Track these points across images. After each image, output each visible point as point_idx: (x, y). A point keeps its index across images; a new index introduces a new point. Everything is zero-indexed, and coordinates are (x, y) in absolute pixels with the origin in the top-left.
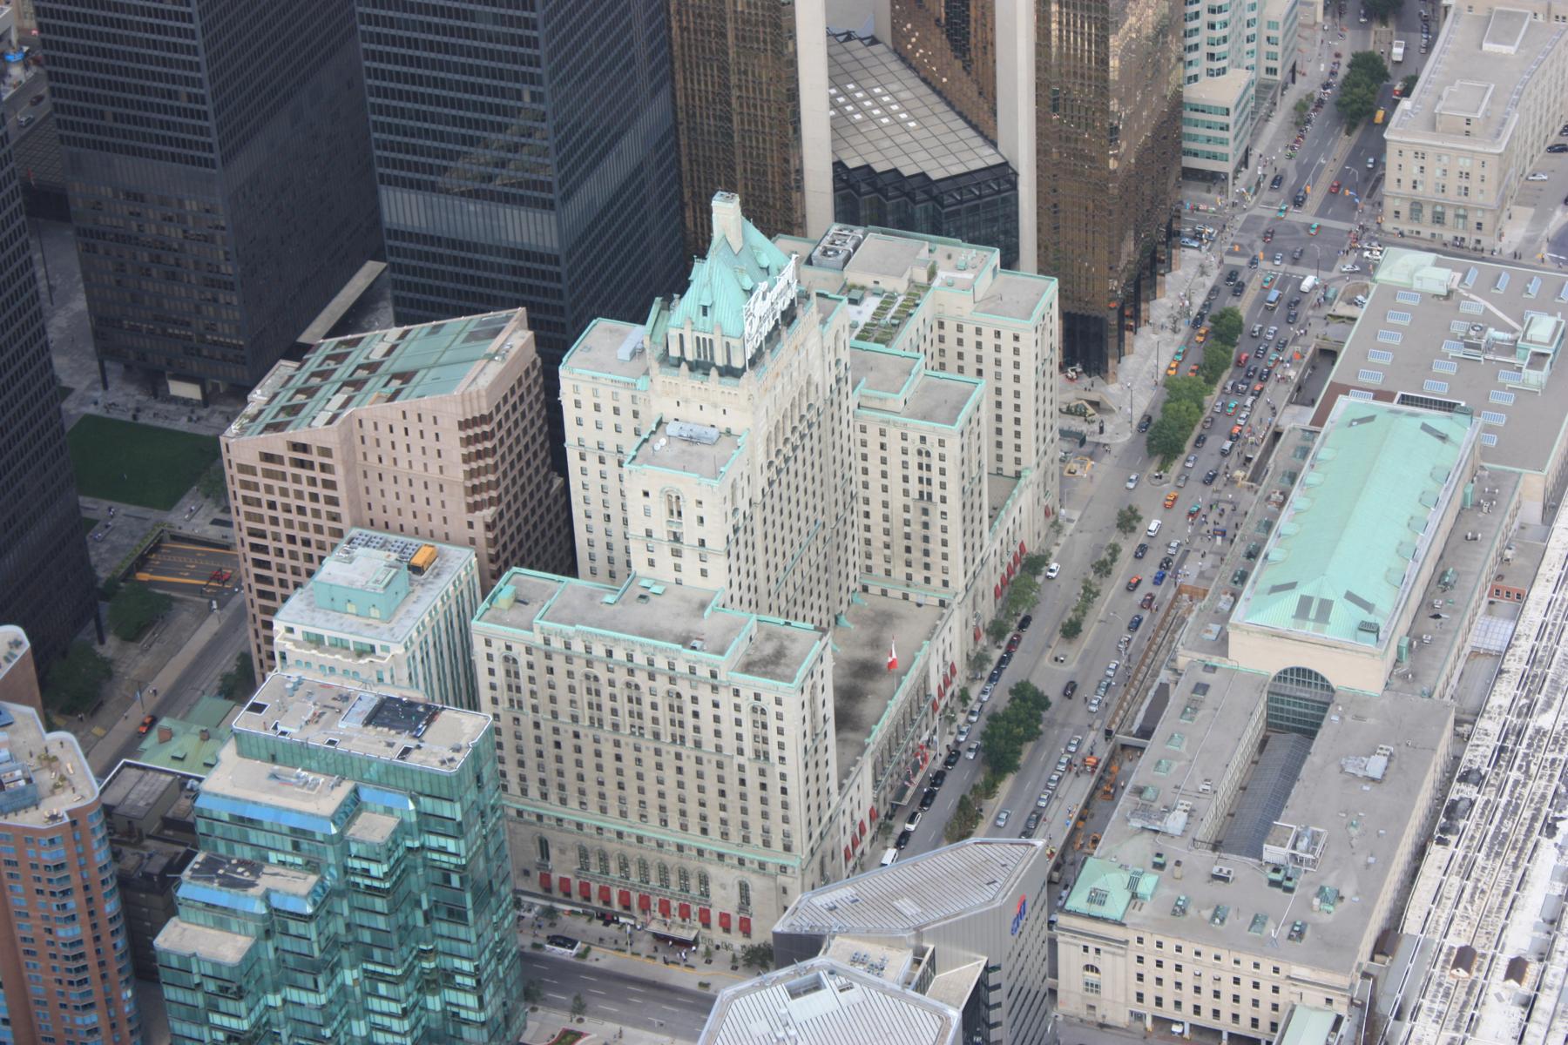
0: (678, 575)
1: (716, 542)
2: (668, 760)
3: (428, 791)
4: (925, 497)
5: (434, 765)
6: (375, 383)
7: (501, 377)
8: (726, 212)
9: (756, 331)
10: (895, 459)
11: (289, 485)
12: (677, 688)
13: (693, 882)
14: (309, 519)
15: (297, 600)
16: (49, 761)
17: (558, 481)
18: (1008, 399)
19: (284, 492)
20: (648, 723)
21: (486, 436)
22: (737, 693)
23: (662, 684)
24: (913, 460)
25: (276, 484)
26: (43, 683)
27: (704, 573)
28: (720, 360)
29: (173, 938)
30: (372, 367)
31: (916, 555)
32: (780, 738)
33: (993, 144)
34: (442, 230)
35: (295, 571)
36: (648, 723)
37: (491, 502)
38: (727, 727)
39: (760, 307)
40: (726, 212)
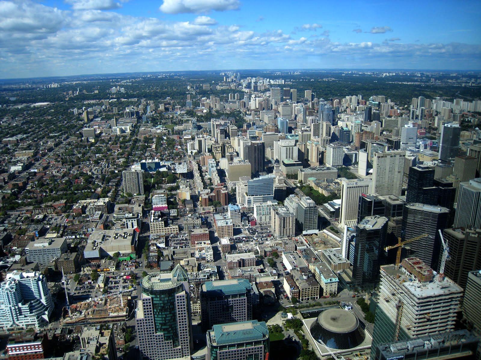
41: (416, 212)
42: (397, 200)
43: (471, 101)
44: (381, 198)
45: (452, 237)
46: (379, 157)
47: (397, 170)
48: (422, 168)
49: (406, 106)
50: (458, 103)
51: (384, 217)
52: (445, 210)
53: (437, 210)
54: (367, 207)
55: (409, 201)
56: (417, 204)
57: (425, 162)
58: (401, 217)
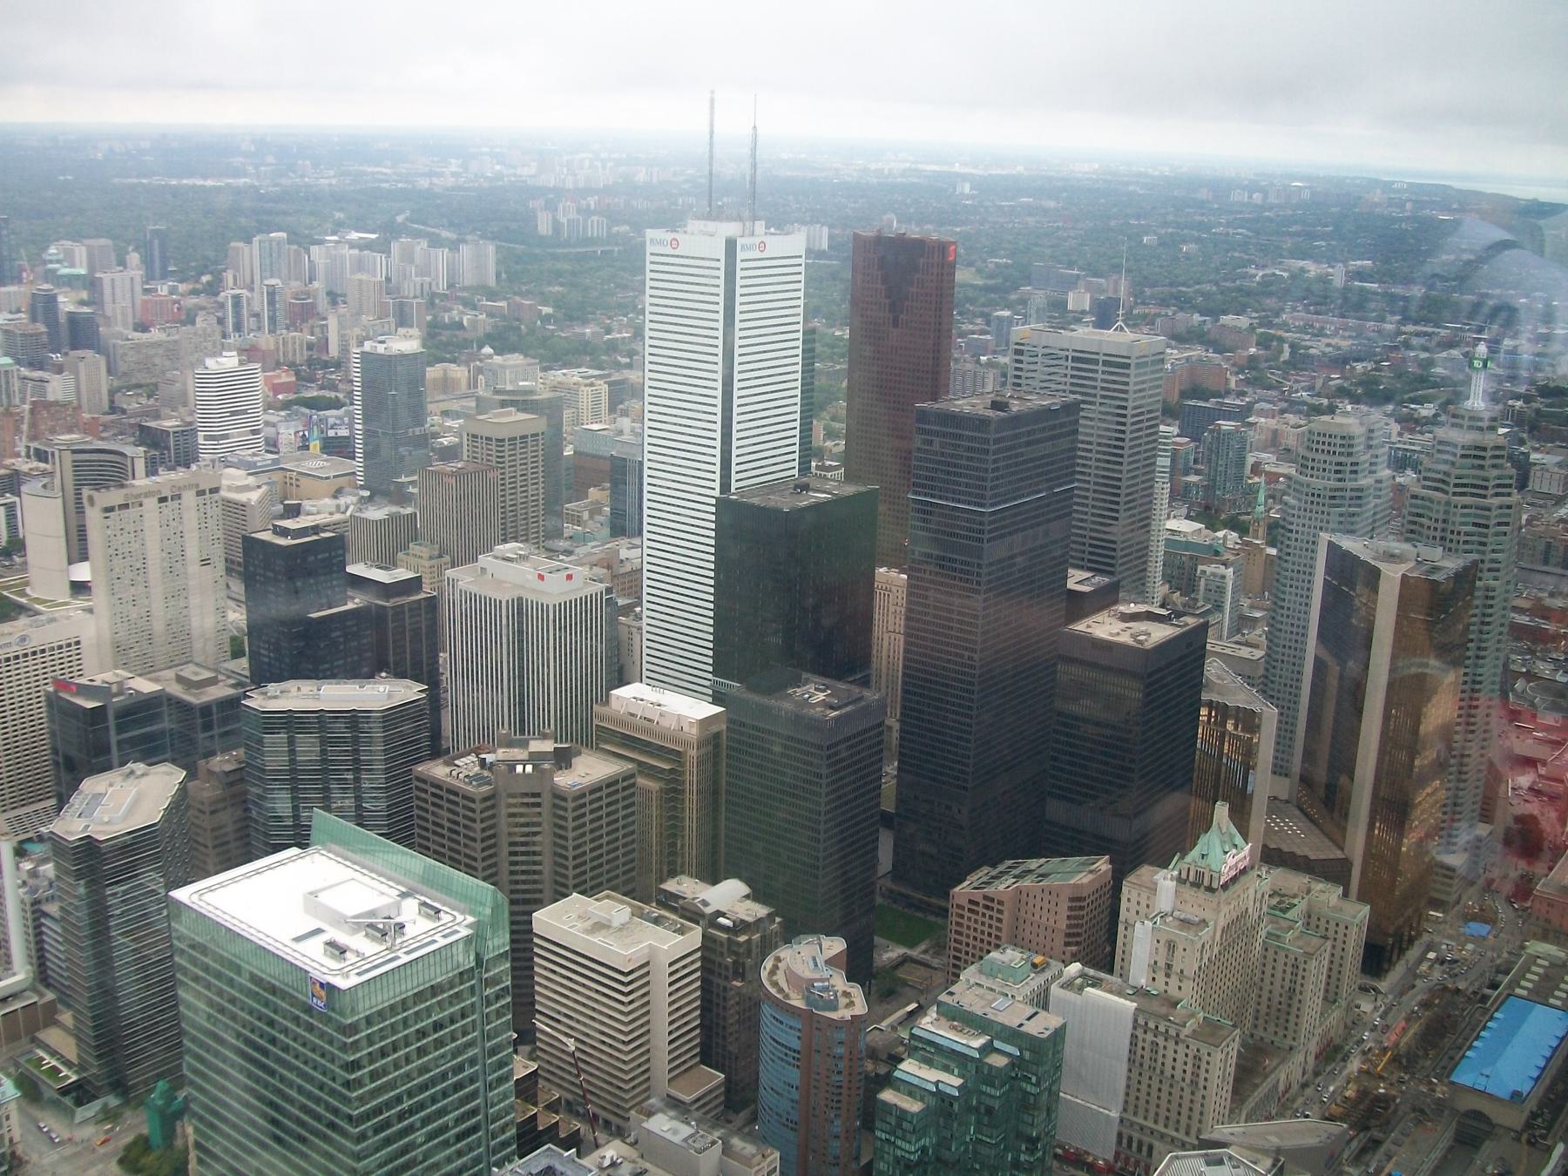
2: (1145, 1081)
4: (1292, 991)
8: (1222, 810)
9: (1226, 873)
10: (1280, 967)
11: (980, 918)
13: (1145, 1149)
14: (986, 937)
15: (972, 969)
16: (846, 994)
18: (1337, 960)
20: (1138, 1058)
21: (1082, 908)
23: (1150, 1037)
24: (1289, 970)
25: (973, 917)
26: (848, 962)
28: (1206, 883)
29: (887, 1096)
30: (1030, 871)
31: (1282, 1021)
33: (1342, 849)
36: (1138, 1058)
38: (1179, 1065)
39: (1231, 862)
40: (1222, 810)
41: (291, 722)
42: (213, 682)
43: (454, 246)
44: (146, 686)
45: (449, 791)
46: (110, 509)
47: (193, 553)
48: (303, 532)
49: (205, 279)
50: (408, 257)
51: (167, 767)
52: (408, 691)
53: (382, 694)
54: (91, 737)
55: (262, 675)
56: (291, 685)
57: (307, 505)
58: (242, 751)
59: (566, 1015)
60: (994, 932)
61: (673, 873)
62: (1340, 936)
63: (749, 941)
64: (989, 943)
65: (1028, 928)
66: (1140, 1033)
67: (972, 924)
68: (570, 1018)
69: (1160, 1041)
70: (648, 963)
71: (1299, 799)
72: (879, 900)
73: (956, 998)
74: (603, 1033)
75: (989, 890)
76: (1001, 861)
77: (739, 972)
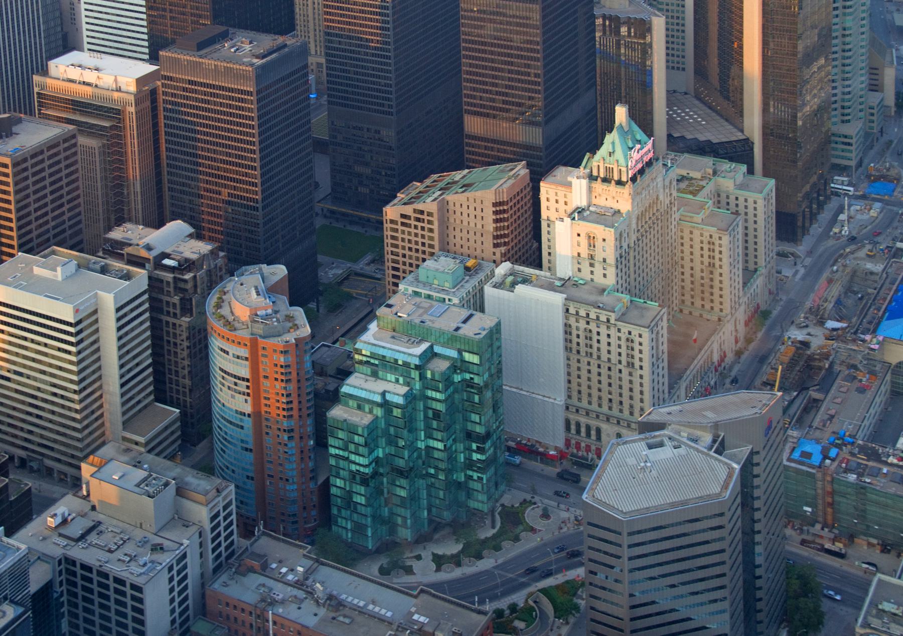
0: (592, 276)
1: (611, 260)
3: (467, 348)
5: (471, 334)
6: (455, 188)
7: (513, 185)
12: (590, 327)
14: (420, 247)
15: (410, 277)
17: (536, 245)
19: (409, 233)
21: (504, 211)
22: (619, 330)
27: (605, 276)
29: (337, 412)
30: (455, 183)
32: (641, 347)
34: (490, 135)
35: (411, 265)
37: (505, 244)
59: (16, 373)
60: (427, 241)
61: (120, 221)
62: (751, 211)
63: (195, 277)
64: (424, 252)
65: (458, 233)
66: (572, 321)
67: (406, 237)
68: (21, 374)
69: (593, 326)
70: (95, 312)
71: (696, 90)
72: (319, 222)
73: (394, 309)
74: (54, 385)
75: (420, 206)
76: (427, 177)
77: (186, 308)
